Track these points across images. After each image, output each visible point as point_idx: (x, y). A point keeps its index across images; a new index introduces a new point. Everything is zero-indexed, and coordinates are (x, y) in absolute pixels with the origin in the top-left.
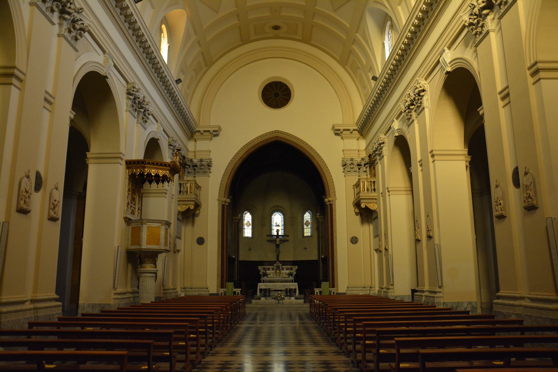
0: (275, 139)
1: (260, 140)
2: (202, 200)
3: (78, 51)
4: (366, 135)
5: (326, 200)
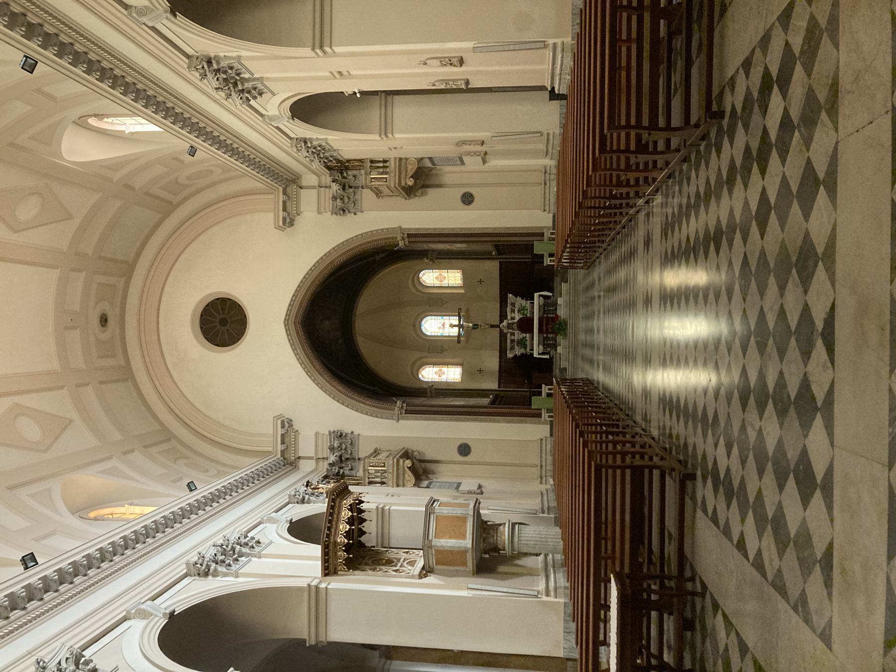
0: (299, 326)
1: (300, 351)
2: (399, 447)
3: (117, 667)
4: (293, 175)
5: (401, 244)
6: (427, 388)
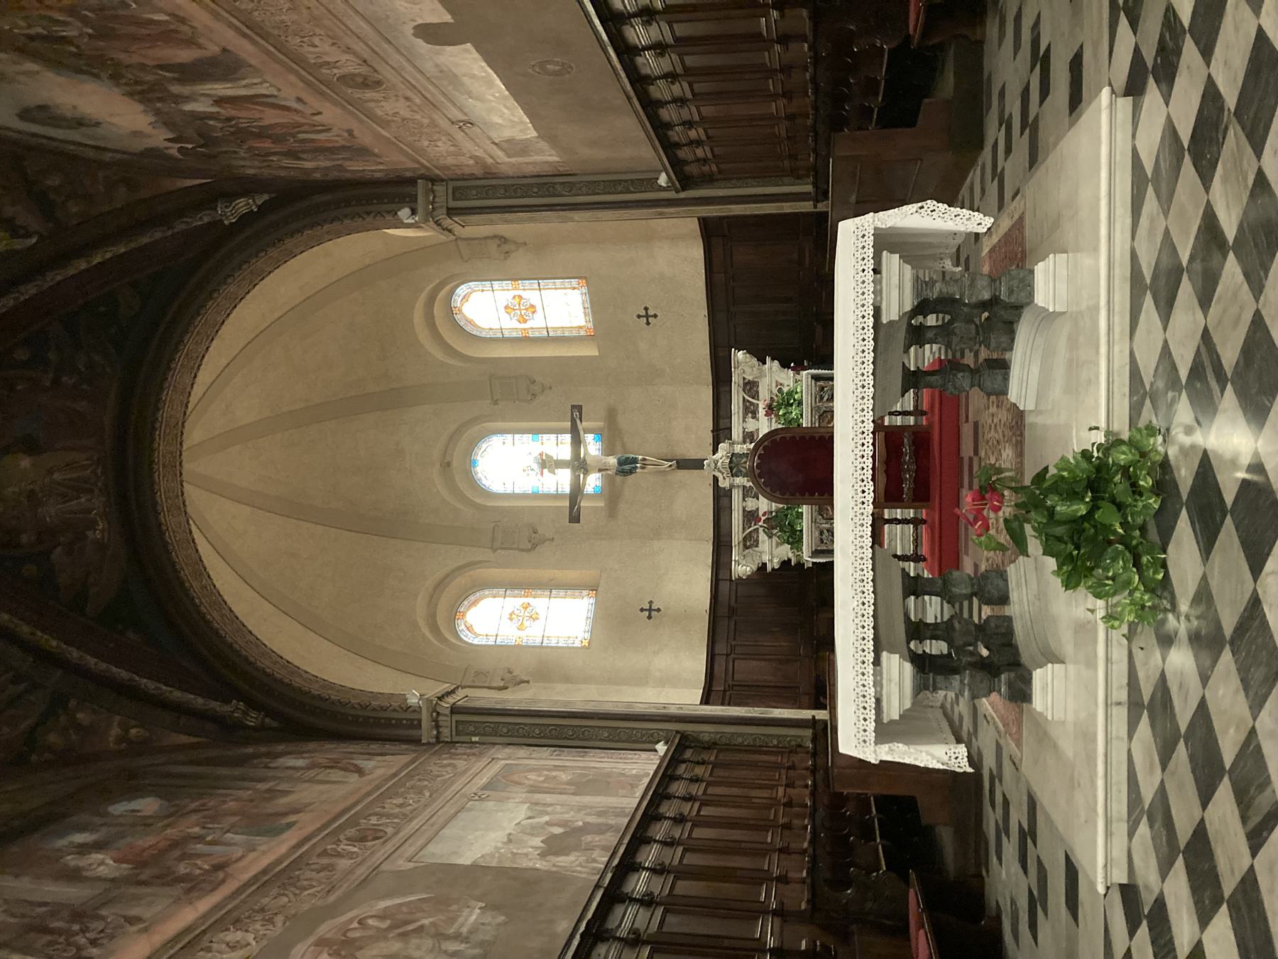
6: (418, 710)
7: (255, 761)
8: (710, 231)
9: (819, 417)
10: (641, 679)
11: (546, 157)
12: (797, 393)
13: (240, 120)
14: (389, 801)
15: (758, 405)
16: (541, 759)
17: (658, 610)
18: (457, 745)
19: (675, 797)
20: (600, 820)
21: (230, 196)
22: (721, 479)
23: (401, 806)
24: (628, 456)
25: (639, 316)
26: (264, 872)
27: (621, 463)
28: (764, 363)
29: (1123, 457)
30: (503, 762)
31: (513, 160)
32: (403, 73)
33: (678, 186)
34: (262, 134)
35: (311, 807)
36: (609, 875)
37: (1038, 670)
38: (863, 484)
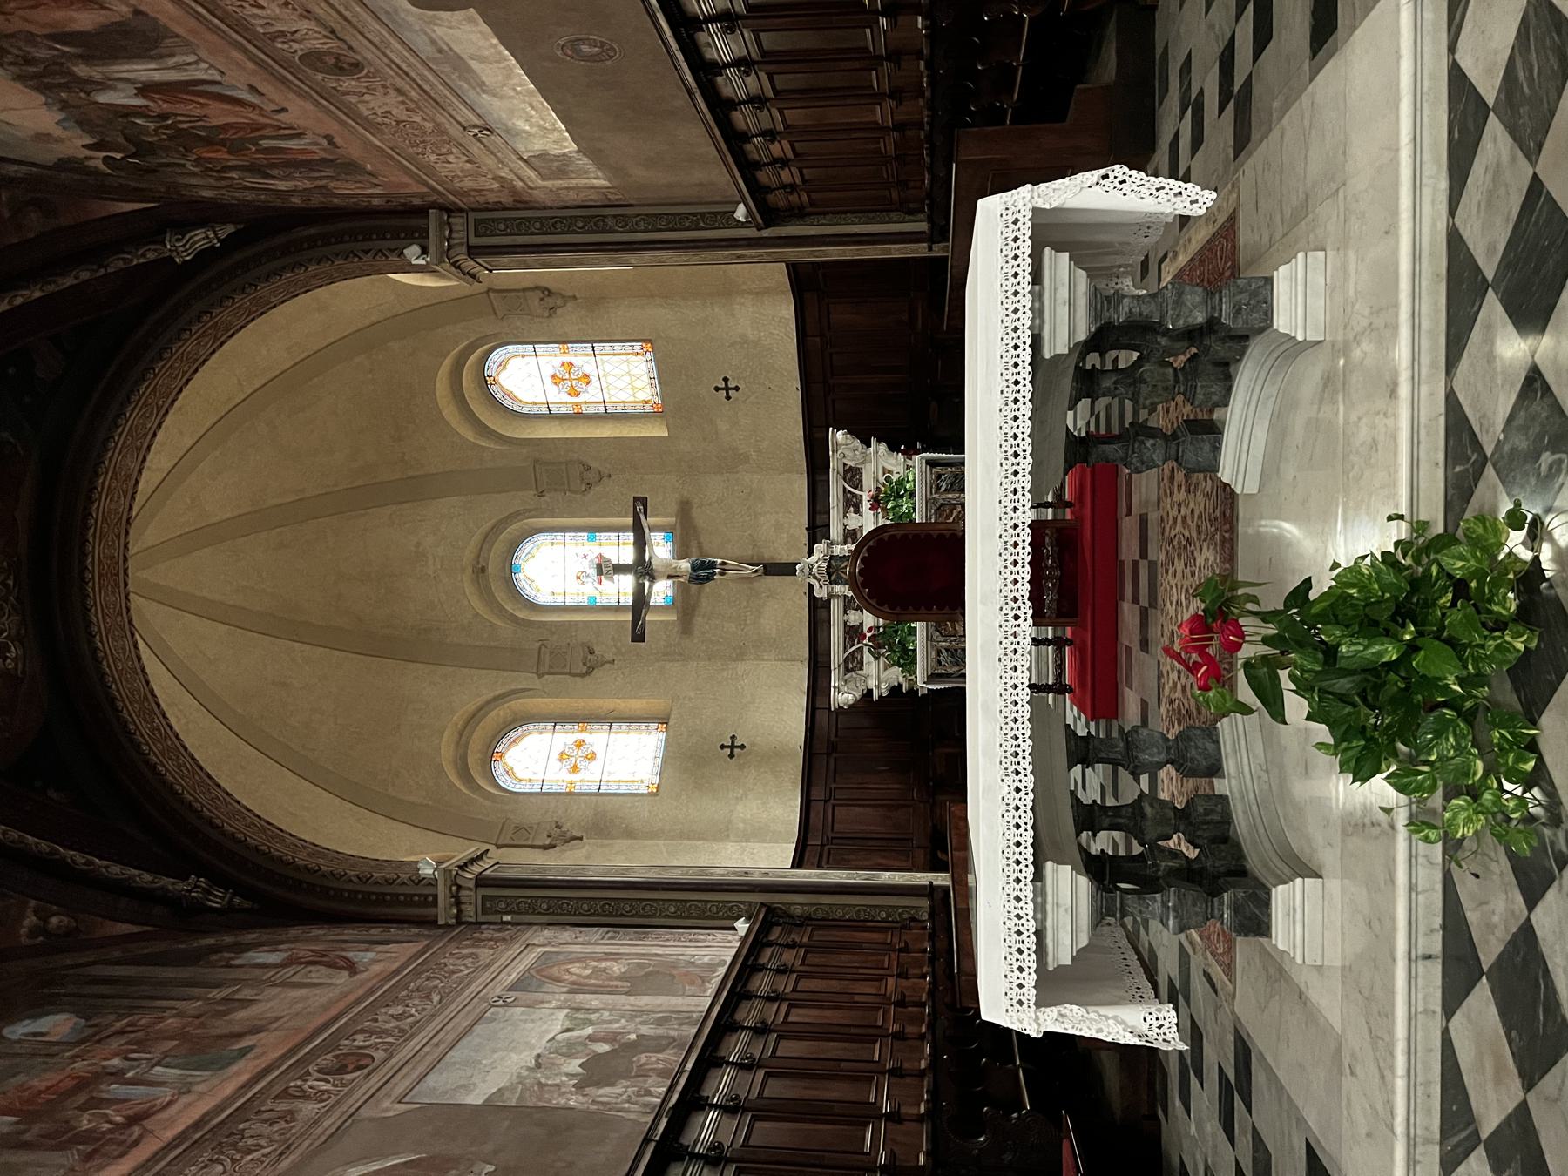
6: (432, 883)
7: (214, 957)
8: (804, 281)
9: (936, 511)
10: (721, 832)
11: (592, 180)
12: (908, 482)
13: (179, 118)
14: (383, 1010)
15: (861, 496)
16: (589, 944)
17: (743, 747)
18: (483, 927)
19: (756, 997)
20: (661, 1031)
21: (183, 227)
22: (817, 587)
23: (398, 1018)
24: (704, 559)
25: (717, 389)
26: (196, 1125)
27: (695, 568)
28: (869, 446)
29: (1460, 564)
30: (539, 950)
31: (549, 184)
32: (388, 52)
33: (760, 220)
34: (213, 138)
35: (275, 1026)
36: (665, 1121)
37: (1280, 887)
38: (1016, 606)
